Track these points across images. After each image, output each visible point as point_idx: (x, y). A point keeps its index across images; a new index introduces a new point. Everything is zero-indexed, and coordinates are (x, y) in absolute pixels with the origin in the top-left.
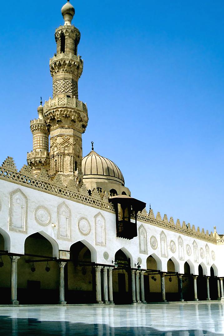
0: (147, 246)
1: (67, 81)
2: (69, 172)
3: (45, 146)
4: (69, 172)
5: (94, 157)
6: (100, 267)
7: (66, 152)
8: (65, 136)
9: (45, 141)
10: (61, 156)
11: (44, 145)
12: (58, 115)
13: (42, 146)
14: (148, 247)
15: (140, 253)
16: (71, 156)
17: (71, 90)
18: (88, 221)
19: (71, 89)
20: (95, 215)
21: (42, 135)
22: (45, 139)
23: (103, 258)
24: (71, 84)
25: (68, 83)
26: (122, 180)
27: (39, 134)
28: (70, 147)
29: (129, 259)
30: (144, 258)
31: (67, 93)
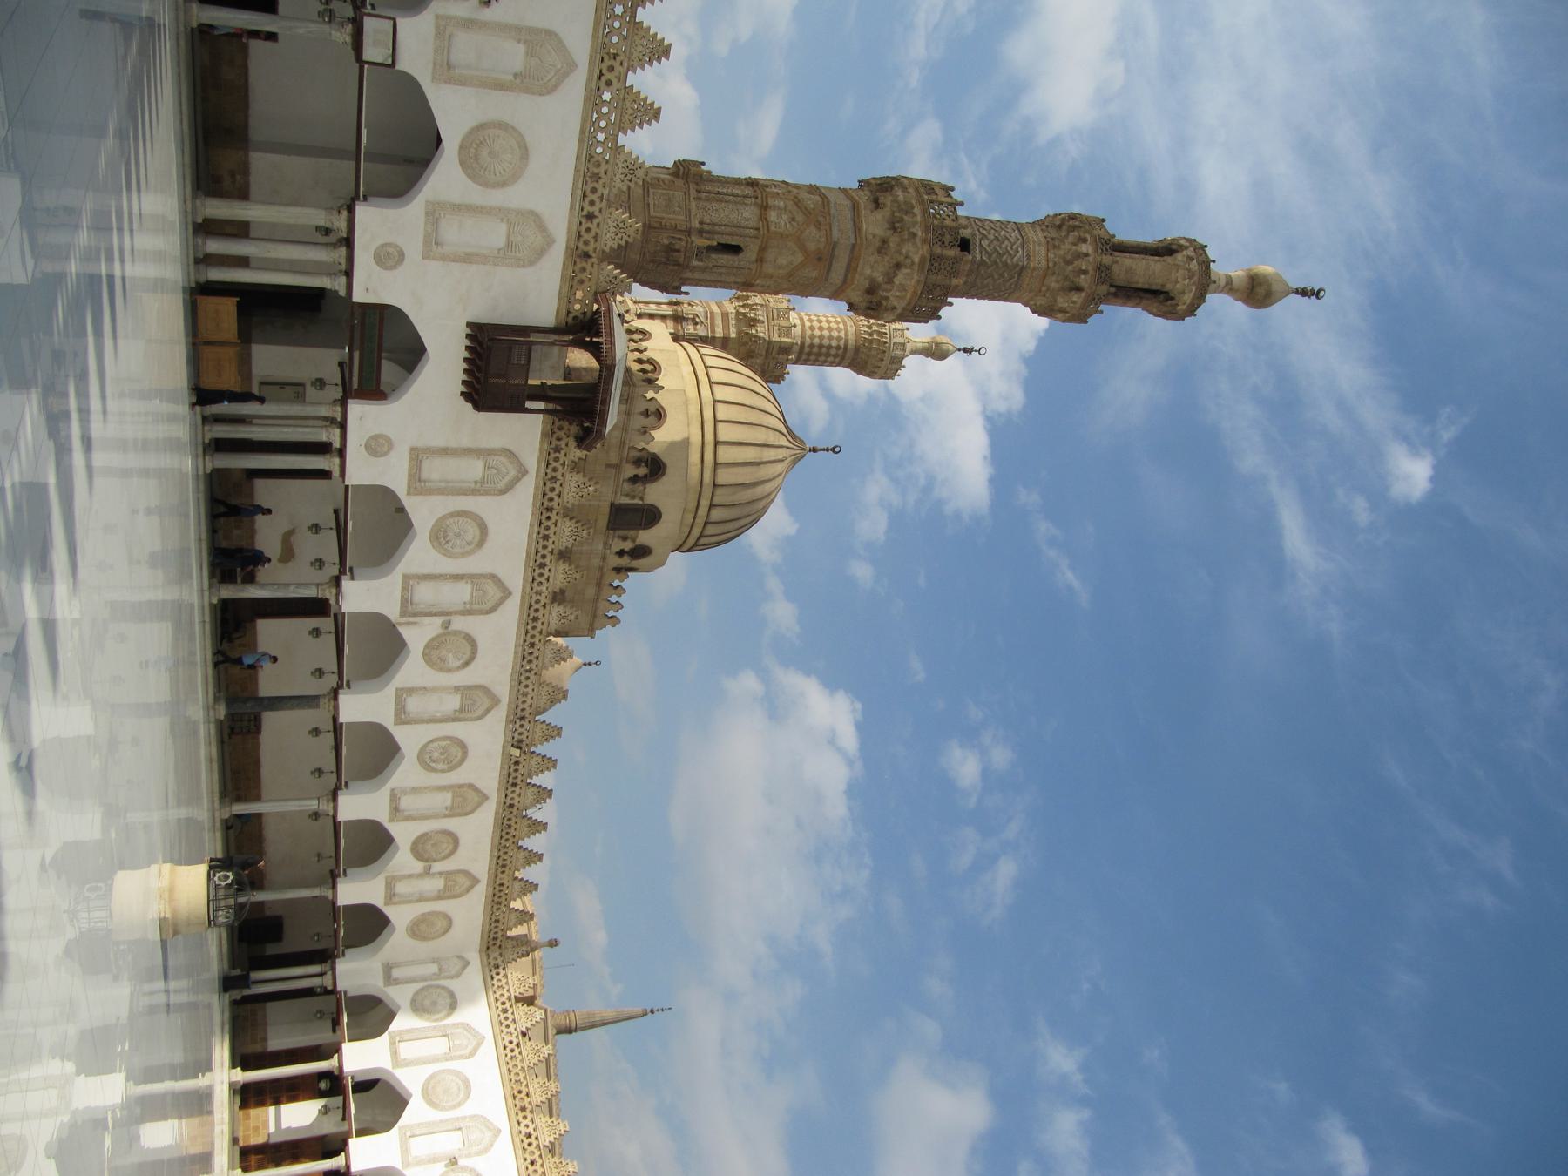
3: (812, 346)
5: (781, 453)
6: (340, 223)
9: (829, 347)
11: (816, 341)
13: (812, 337)
15: (413, 449)
18: (501, 86)
21: (852, 338)
22: (838, 347)
26: (701, 536)
27: (852, 330)
30: (393, 474)
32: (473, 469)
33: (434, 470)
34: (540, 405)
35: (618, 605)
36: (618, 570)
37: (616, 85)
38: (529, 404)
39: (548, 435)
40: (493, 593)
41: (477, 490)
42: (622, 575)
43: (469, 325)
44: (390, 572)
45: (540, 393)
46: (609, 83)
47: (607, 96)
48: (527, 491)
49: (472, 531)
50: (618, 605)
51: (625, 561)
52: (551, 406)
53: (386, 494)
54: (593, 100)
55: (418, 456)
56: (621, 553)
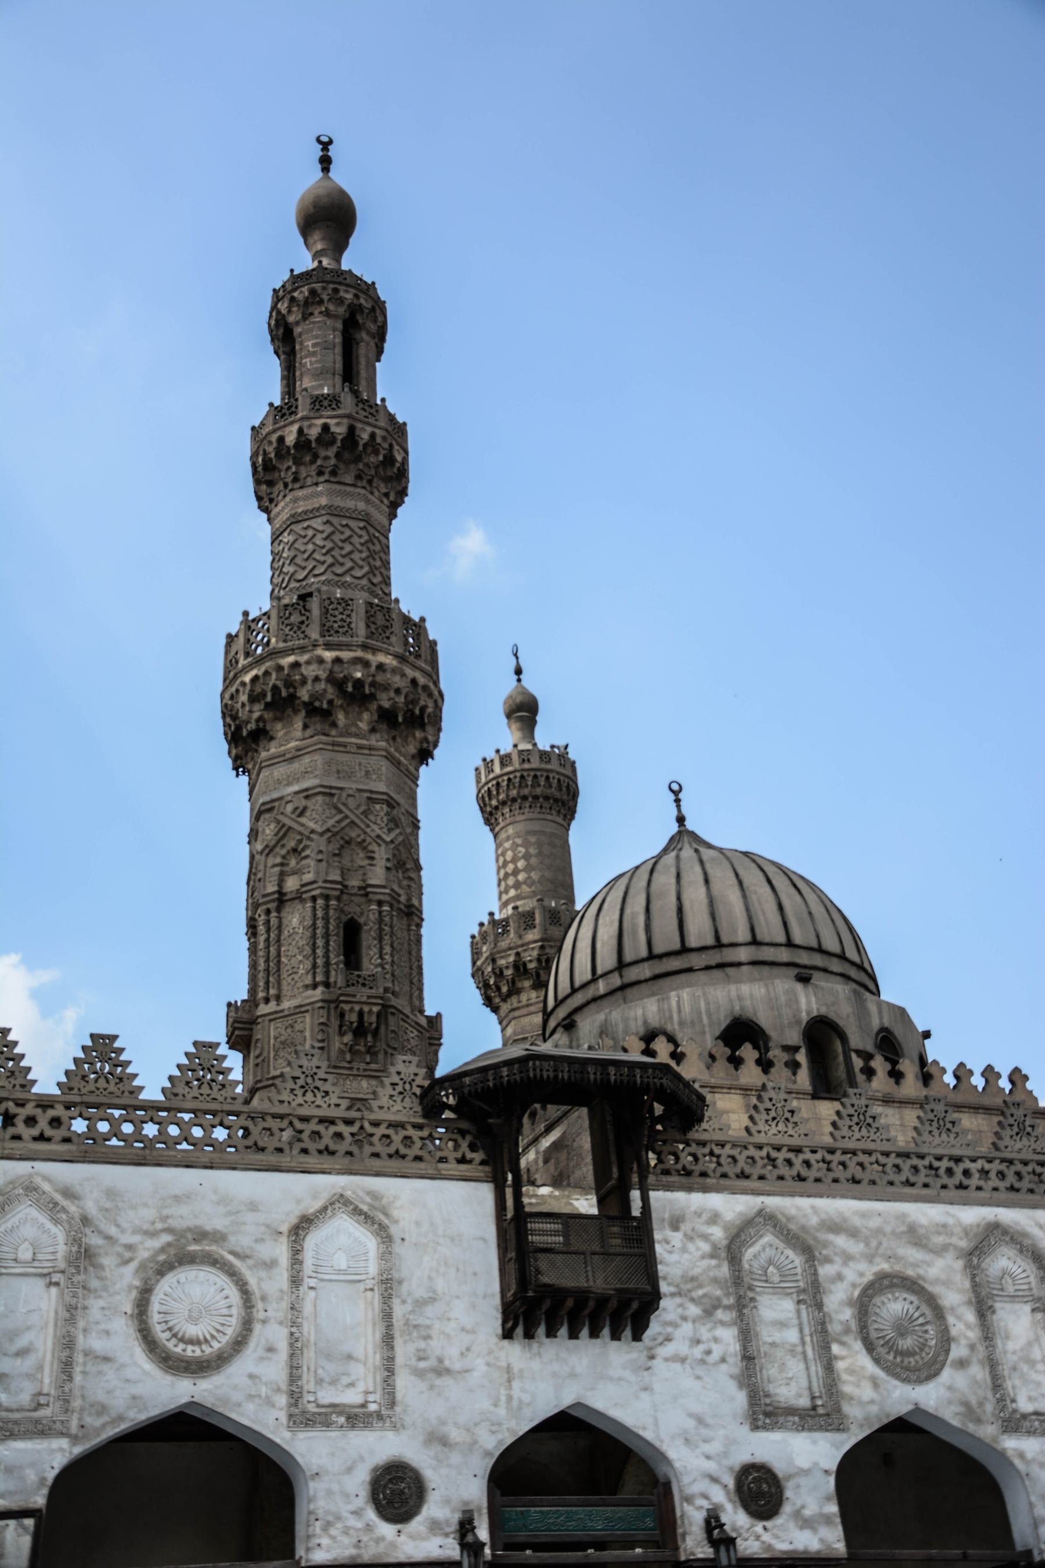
0: (829, 1367)
1: (344, 522)
2: (306, 987)
4: (306, 987)
7: (291, 884)
8: (283, 802)
10: (268, 912)
12: (243, 705)
14: (840, 1365)
15: (755, 1428)
16: (314, 899)
17: (361, 567)
19: (361, 563)
20: (294, 1220)
23: (371, 1514)
24: (360, 536)
25: (348, 533)
28: (307, 852)
29: (667, 1485)
30: (810, 1459)
31: (304, 583)
32: (777, 1314)
33: (791, 1382)
34: (635, 1195)
35: (990, 1073)
36: (926, 1078)
37: (59, 1111)
38: (636, 1211)
39: (692, 1178)
40: (1004, 1262)
41: (812, 1295)
42: (933, 1070)
43: (507, 1335)
44: (1002, 1455)
45: (612, 1195)
46: (55, 1122)
47: (79, 1126)
48: (804, 1208)
49: (895, 1306)
50: (990, 1073)
51: (908, 1067)
52: (635, 1178)
53: (851, 1474)
54: (91, 1150)
55: (764, 1413)
56: (896, 1075)
